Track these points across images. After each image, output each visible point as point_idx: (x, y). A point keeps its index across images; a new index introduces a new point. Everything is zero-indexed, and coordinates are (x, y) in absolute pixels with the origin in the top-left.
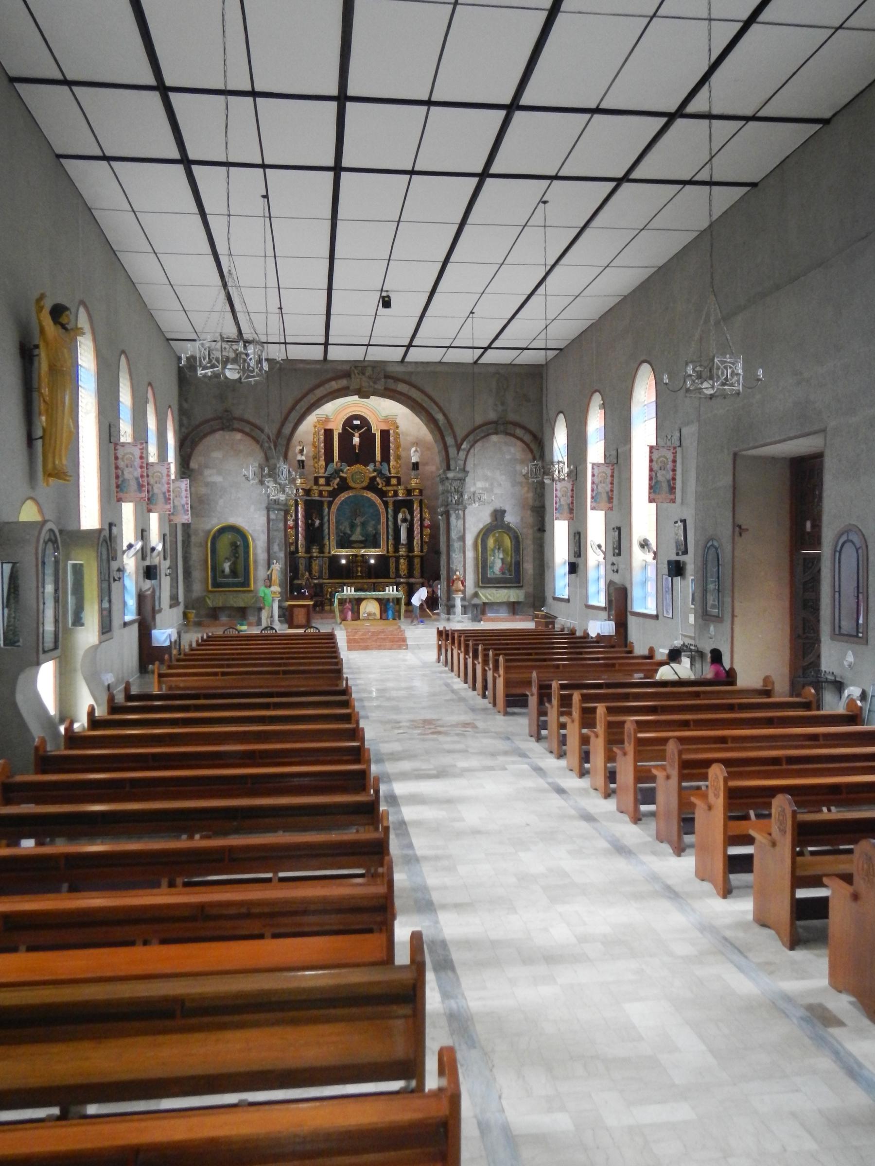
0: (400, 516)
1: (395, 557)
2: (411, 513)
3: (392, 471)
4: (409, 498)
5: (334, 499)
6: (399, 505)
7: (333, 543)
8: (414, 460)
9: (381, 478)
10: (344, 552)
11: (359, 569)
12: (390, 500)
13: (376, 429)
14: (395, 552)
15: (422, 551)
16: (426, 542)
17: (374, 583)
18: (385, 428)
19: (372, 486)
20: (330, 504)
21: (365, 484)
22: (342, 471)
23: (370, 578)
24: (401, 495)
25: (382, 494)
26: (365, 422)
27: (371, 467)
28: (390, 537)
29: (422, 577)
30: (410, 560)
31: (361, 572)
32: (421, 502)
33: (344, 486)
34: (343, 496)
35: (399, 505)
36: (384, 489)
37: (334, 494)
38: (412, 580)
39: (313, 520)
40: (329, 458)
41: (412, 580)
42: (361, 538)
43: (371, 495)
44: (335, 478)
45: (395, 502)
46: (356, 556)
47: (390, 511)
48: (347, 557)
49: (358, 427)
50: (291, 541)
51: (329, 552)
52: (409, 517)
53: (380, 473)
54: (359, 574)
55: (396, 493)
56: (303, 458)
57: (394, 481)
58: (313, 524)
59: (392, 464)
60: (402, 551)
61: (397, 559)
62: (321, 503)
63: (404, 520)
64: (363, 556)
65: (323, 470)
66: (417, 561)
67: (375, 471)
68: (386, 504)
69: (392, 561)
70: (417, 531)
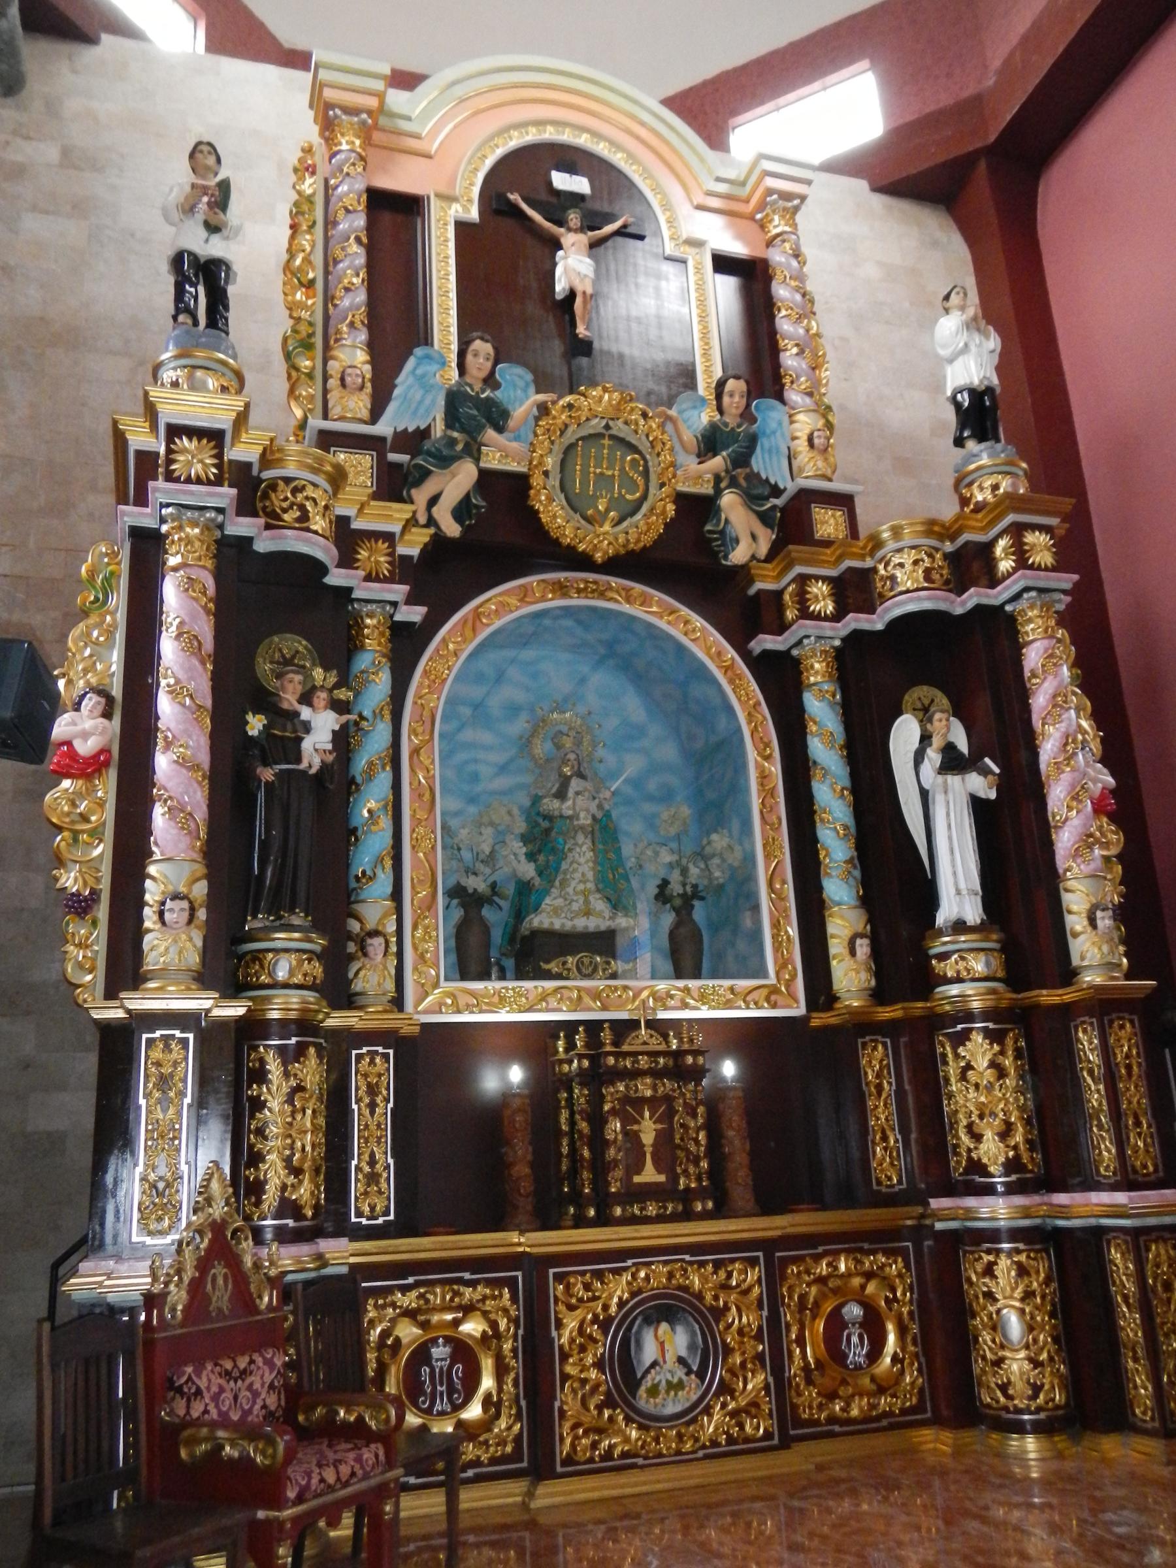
4: (963, 604)
6: (881, 672)
7: (430, 936)
10: (508, 1003)
12: (815, 640)
14: (879, 995)
17: (768, 1245)
22: (497, 416)
30: (1037, 1037)
31: (668, 1151)
33: (501, 538)
34: (501, 605)
35: (881, 672)
37: (449, 573)
38: (1084, 1207)
39: (282, 717)
40: (396, 325)
41: (1084, 1207)
44: (445, 461)
45: (852, 657)
48: (535, 1042)
50: (70, 880)
54: (649, 1175)
55: (855, 590)
56: (215, 248)
57: (828, 523)
58: (285, 740)
61: (922, 1045)
65: (360, 404)
69: (874, 1060)
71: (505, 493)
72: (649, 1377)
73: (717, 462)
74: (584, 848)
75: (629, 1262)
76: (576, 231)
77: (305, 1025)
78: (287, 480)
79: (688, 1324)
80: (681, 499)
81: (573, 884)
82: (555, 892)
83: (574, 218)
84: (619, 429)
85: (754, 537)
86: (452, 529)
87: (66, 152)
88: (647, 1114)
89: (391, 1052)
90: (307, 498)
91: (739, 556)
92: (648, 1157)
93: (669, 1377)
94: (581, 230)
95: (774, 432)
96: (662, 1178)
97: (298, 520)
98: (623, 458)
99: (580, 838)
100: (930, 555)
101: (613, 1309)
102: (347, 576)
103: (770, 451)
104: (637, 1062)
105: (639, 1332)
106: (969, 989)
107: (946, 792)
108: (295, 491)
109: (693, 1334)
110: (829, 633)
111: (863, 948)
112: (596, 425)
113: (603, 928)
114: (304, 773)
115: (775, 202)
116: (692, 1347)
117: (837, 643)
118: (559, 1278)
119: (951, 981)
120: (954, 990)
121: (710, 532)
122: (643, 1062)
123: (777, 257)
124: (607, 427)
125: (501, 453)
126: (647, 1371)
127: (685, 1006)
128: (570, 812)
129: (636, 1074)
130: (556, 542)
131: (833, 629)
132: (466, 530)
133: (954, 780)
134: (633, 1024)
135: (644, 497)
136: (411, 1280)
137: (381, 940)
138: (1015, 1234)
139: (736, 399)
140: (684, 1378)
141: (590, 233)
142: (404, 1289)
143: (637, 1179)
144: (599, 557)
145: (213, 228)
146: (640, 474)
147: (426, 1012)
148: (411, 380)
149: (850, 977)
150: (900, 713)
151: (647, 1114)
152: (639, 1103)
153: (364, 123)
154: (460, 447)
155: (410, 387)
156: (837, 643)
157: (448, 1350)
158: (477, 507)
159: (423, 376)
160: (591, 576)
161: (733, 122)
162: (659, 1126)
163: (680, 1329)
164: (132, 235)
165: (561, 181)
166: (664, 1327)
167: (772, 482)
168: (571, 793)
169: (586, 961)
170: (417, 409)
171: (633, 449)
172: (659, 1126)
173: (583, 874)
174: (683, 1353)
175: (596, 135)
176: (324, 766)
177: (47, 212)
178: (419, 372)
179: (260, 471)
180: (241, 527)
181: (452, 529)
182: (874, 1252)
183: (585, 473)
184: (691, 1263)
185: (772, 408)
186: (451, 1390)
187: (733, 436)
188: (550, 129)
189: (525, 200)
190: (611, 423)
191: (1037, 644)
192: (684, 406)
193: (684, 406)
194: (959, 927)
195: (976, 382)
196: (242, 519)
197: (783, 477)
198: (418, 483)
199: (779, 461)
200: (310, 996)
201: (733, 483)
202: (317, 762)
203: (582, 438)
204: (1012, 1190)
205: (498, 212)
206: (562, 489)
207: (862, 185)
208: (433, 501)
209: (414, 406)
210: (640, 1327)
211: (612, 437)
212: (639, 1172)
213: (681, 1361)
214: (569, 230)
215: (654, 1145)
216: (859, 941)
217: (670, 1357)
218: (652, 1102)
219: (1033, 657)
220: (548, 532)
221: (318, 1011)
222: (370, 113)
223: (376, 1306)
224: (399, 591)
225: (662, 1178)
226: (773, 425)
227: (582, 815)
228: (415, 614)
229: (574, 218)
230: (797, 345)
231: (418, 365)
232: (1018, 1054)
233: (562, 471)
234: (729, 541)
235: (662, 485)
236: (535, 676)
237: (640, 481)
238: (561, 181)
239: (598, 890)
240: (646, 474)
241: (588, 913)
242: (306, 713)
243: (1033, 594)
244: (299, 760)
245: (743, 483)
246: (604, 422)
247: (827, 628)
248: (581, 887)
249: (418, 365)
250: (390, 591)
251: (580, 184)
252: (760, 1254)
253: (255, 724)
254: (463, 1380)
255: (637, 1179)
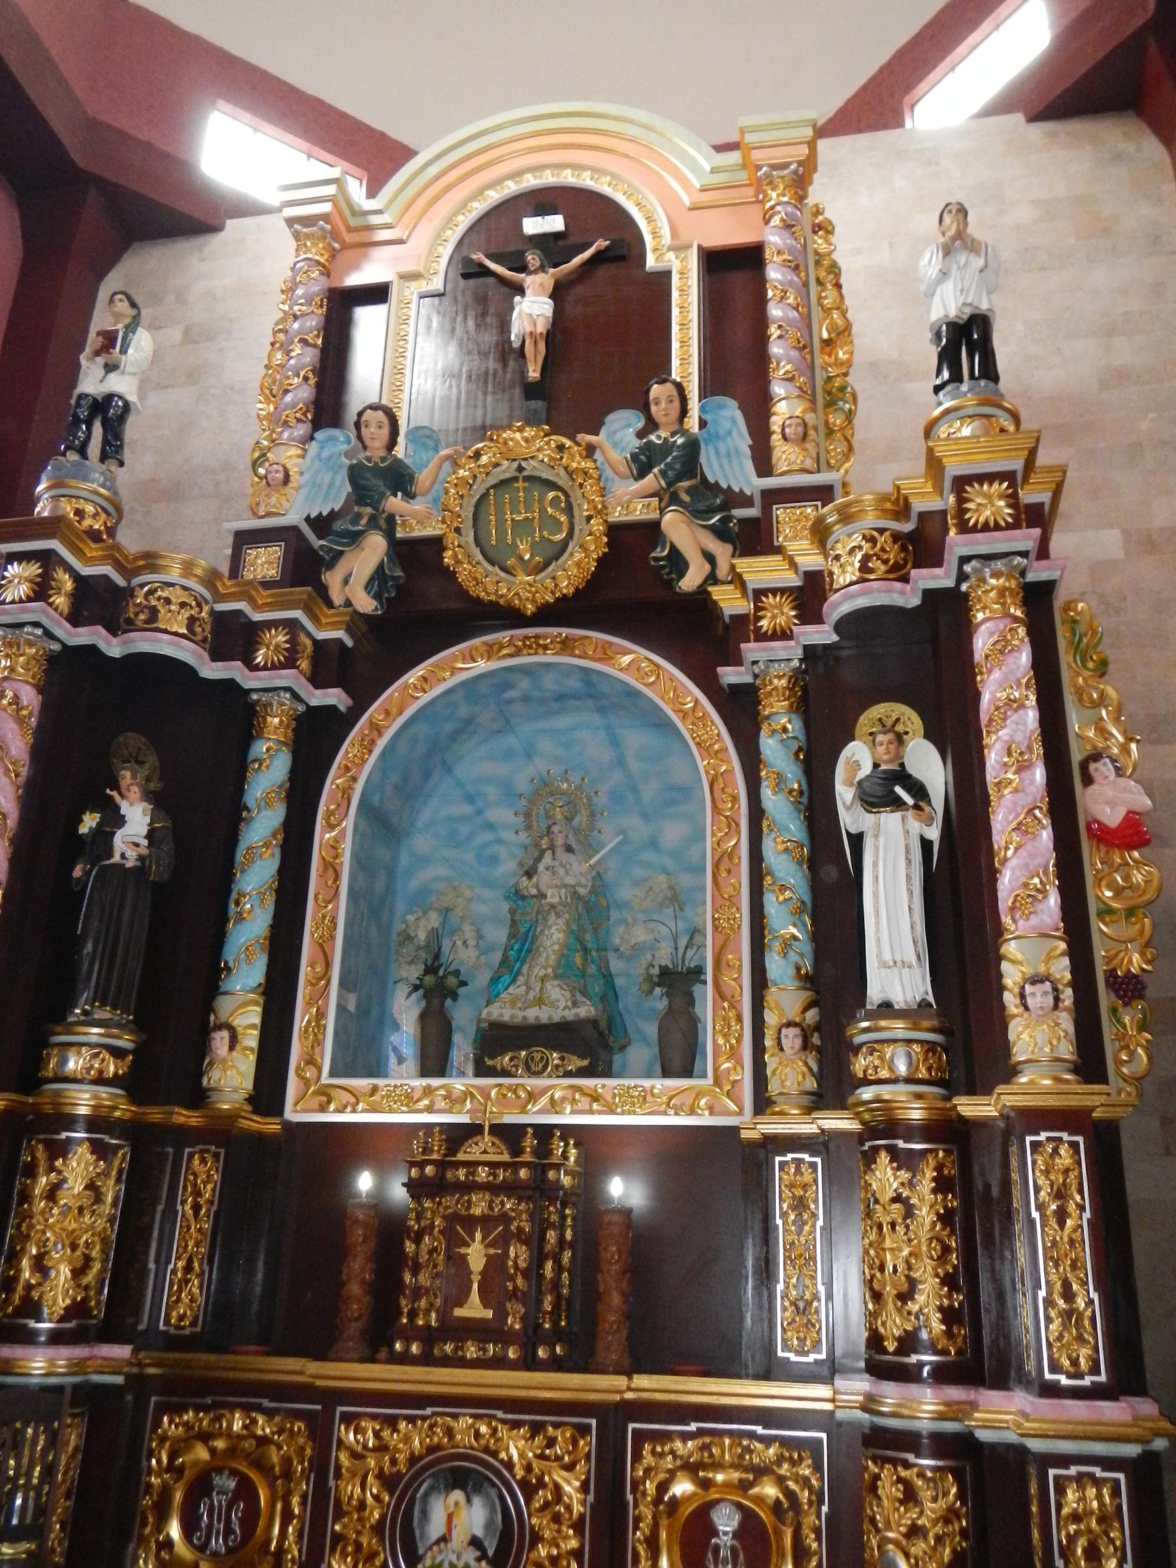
0: (858, 758)
1: (820, 1144)
2: (958, 730)
3: (784, 454)
5: (362, 700)
8: (948, 304)
9: (698, 513)
11: (476, 1255)
12: (771, 663)
13: (672, 252)
15: (1090, 1062)
16: (1129, 988)
18: (728, 233)
19: (631, 591)
20: (316, 739)
21: (569, 574)
23: (582, 1359)
24: (856, 588)
25: (698, 635)
26: (592, 212)
27: (620, 433)
28: (777, 966)
29: (1127, 1375)
32: (1038, 601)
33: (424, 608)
36: (730, 602)
42: (559, 1005)
43: (632, 663)
44: (355, 538)
46: (458, 1135)
47: (771, 747)
49: (552, 248)
51: (268, 1091)
52: (929, 766)
53: (679, 469)
54: (474, 1309)
55: (810, 595)
57: (790, 523)
59: (785, 408)
60: (894, 1071)
62: (237, 714)
63: (890, 789)
64: (510, 1135)
66: (1047, 1183)
67: (642, 464)
68: (741, 710)
70: (1022, 858)
71: (417, 558)
72: (429, 1554)
73: (651, 481)
74: (553, 930)
75: (429, 1411)
76: (535, 272)
77: (95, 1123)
78: (142, 586)
79: (488, 1496)
80: (615, 531)
81: (536, 971)
82: (521, 979)
83: (532, 259)
84: (530, 467)
85: (710, 558)
86: (366, 604)
87: (187, 332)
88: (478, 1236)
89: (222, 1151)
90: (159, 599)
91: (690, 582)
92: (475, 1286)
93: (454, 1558)
94: (542, 269)
95: (730, 433)
96: (489, 1314)
97: (148, 621)
98: (541, 501)
99: (552, 918)
100: (872, 540)
101: (403, 1468)
102: (226, 669)
103: (728, 455)
104: (474, 1174)
105: (426, 1495)
106: (886, 1092)
107: (876, 836)
108: (151, 592)
109: (493, 1510)
110: (783, 655)
111: (791, 1039)
112: (507, 469)
113: (556, 1019)
114: (120, 866)
115: (767, 175)
116: (489, 1525)
117: (796, 663)
118: (347, 1419)
119: (866, 1082)
120: (867, 1093)
121: (656, 559)
122: (482, 1174)
123: (774, 239)
124: (520, 469)
125: (417, 517)
126: (430, 1548)
127: (591, 1112)
128: (534, 891)
129: (470, 1187)
130: (478, 600)
131: (785, 648)
132: (390, 605)
133: (891, 820)
134: (473, 1130)
135: (570, 534)
136: (209, 1401)
137: (225, 1034)
138: (942, 1444)
139: (663, 405)
140: (473, 1563)
141: (552, 270)
142: (197, 1410)
143: (458, 1312)
144: (530, 609)
145: (110, 368)
146: (563, 511)
147: (305, 1111)
148: (317, 463)
149: (791, 1073)
150: (853, 739)
151: (478, 1236)
152: (470, 1222)
153: (322, 229)
154: (364, 521)
155: (316, 473)
156: (796, 663)
157: (232, 1484)
158: (394, 578)
159: (330, 458)
160: (531, 631)
161: (907, 100)
162: (492, 1251)
163: (477, 1501)
164: (232, 389)
165: (533, 226)
166: (457, 1495)
167: (737, 489)
168: (541, 867)
169: (537, 1056)
170: (327, 493)
171: (553, 486)
172: (492, 1251)
173: (547, 958)
174: (479, 1532)
175: (577, 167)
176: (141, 858)
177: (167, 387)
178: (325, 455)
179: (129, 582)
180: (83, 636)
181: (366, 604)
182: (767, 1441)
183: (501, 522)
184: (504, 1422)
185: (721, 407)
186: (228, 1531)
187: (667, 447)
188: (529, 176)
189: (490, 257)
190: (524, 464)
191: (983, 627)
192: (615, 426)
193: (615, 426)
194: (886, 1008)
195: (953, 313)
196: (80, 630)
197: (749, 482)
198: (331, 565)
199: (741, 464)
200: (104, 1092)
201: (675, 499)
202: (132, 854)
203: (494, 487)
204: (943, 1375)
205: (466, 276)
206: (477, 542)
207: (1019, 118)
208: (346, 581)
209: (325, 488)
210: (426, 1495)
211: (527, 479)
212: (461, 1301)
213: (475, 1542)
214: (530, 273)
215: (482, 1273)
216: (784, 1031)
217: (459, 1537)
218: (486, 1222)
219: (981, 643)
220: (467, 592)
221: (115, 1108)
222: (325, 217)
223: (171, 1422)
224: (286, 677)
225: (489, 1314)
226: (727, 425)
227: (549, 894)
228: (334, 697)
229: (532, 259)
230: (780, 327)
231: (322, 448)
232: (942, 1185)
233: (475, 525)
234: (678, 563)
235: (589, 518)
236: (567, 746)
237: (563, 518)
238: (533, 226)
239: (556, 977)
240: (569, 510)
241: (540, 1002)
242: (125, 808)
243: (974, 563)
244: (110, 855)
245: (686, 498)
246: (516, 464)
247: (779, 649)
248: (543, 972)
249: (322, 448)
250: (281, 677)
251: (555, 223)
252: (631, 1426)
253: (89, 822)
254: (242, 1522)
255: (458, 1312)
